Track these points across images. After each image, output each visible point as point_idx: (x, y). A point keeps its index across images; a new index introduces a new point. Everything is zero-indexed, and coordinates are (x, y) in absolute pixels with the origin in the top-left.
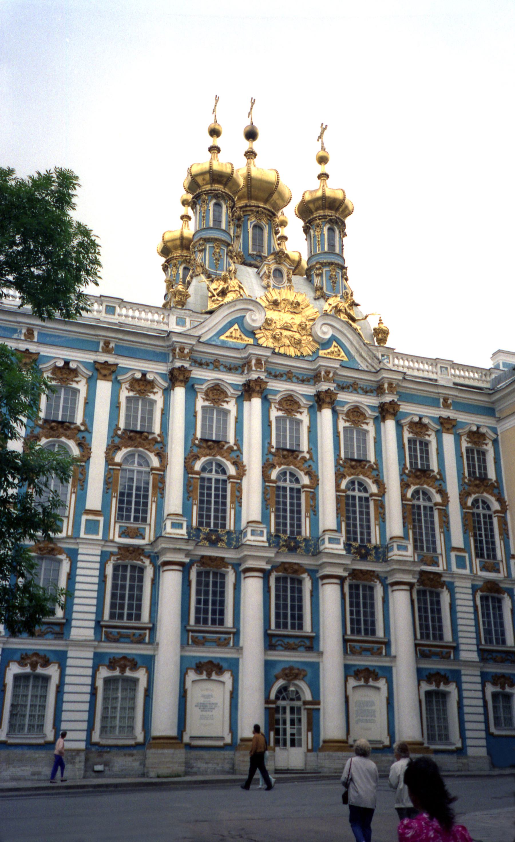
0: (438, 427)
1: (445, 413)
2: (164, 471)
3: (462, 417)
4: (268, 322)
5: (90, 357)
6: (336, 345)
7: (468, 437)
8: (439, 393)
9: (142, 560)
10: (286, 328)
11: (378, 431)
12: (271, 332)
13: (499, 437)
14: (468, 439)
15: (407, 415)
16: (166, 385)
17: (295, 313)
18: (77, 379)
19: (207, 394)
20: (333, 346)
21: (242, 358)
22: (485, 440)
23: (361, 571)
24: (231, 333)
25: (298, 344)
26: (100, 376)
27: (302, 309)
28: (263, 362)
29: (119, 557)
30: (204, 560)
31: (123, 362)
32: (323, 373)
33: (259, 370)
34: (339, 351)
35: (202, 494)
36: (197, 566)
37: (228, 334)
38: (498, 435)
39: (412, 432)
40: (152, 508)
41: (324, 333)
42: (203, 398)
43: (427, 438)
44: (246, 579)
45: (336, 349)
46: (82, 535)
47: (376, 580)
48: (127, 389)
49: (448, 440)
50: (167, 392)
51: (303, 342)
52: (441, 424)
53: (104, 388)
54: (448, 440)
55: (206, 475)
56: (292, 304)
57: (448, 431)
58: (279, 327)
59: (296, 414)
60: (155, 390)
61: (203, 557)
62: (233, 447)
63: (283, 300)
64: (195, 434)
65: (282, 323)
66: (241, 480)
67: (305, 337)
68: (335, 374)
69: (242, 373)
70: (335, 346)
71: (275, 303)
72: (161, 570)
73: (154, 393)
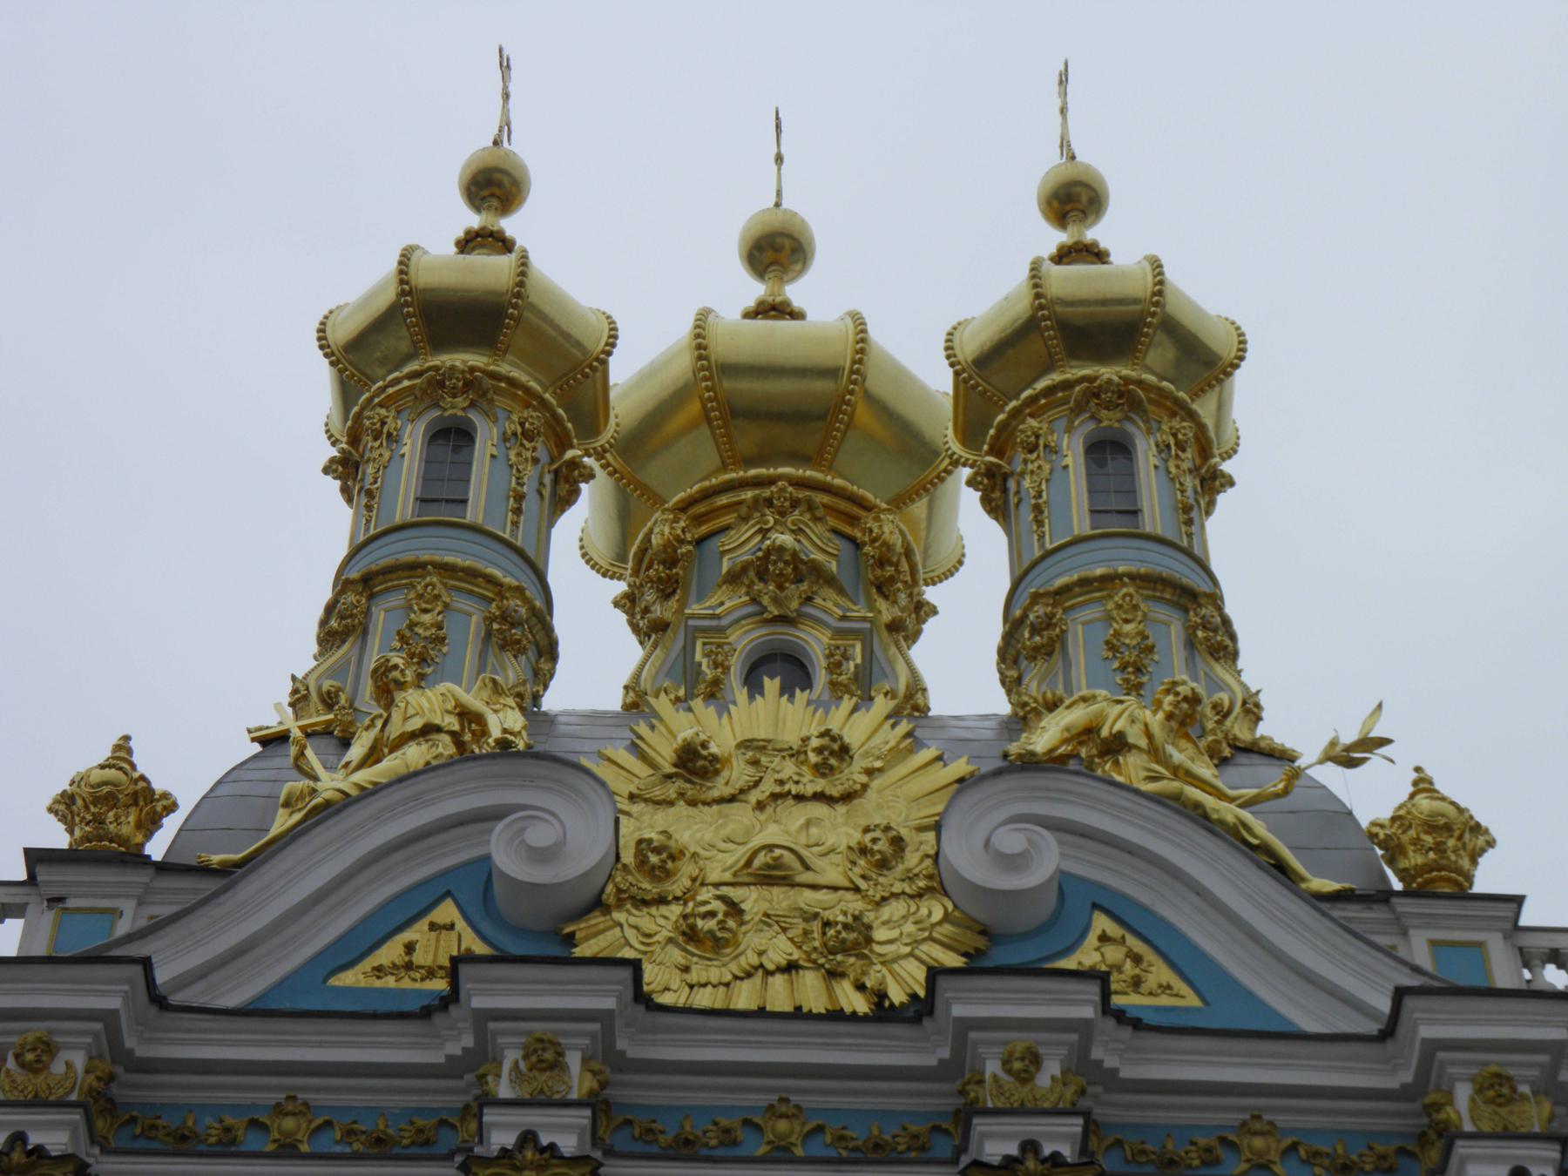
4: (658, 860)
6: (1113, 929)
10: (772, 875)
12: (675, 910)
17: (820, 797)
20: (1092, 939)
24: (410, 948)
25: (845, 948)
27: (870, 772)
32: (992, 1067)
34: (1137, 959)
37: (390, 953)
45: (1114, 954)
51: (880, 934)
56: (797, 754)
58: (714, 876)
63: (745, 745)
65: (739, 854)
67: (896, 908)
68: (1082, 1068)
70: (1104, 938)
71: (694, 764)
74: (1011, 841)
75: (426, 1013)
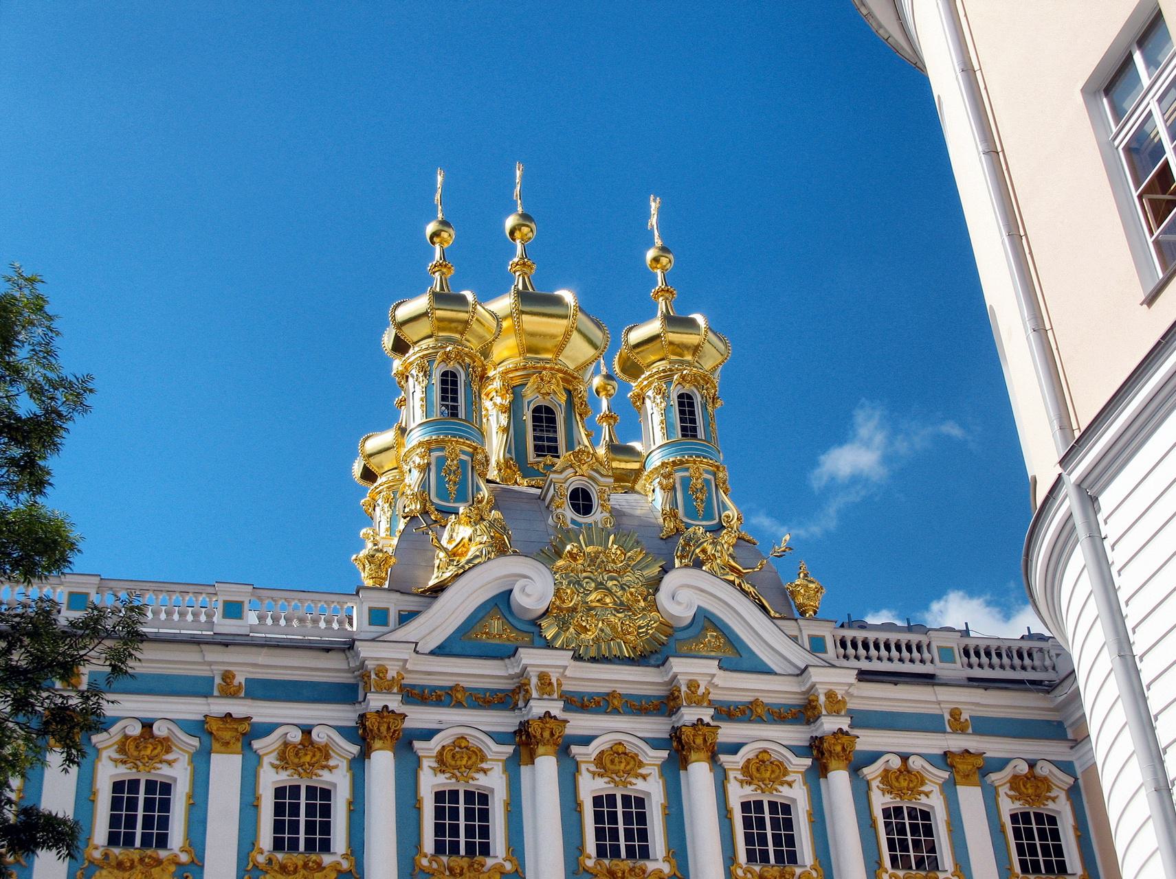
0: (946, 775)
1: (956, 743)
3: (994, 747)
5: (192, 709)
7: (1011, 788)
13: (1080, 781)
14: (1012, 793)
15: (873, 757)
16: (355, 749)
18: (170, 757)
19: (440, 759)
21: (511, 677)
22: (1049, 789)
26: (216, 746)
28: (554, 680)
31: (262, 712)
33: (545, 696)
38: (1076, 779)
42: (433, 769)
43: (923, 799)
48: (273, 765)
49: (970, 798)
50: (358, 764)
52: (952, 766)
54: (970, 798)
57: (967, 779)
59: (634, 781)
60: (331, 763)
62: (502, 866)
64: (418, 846)
69: (515, 707)
73: (330, 769)
75: (502, 659)
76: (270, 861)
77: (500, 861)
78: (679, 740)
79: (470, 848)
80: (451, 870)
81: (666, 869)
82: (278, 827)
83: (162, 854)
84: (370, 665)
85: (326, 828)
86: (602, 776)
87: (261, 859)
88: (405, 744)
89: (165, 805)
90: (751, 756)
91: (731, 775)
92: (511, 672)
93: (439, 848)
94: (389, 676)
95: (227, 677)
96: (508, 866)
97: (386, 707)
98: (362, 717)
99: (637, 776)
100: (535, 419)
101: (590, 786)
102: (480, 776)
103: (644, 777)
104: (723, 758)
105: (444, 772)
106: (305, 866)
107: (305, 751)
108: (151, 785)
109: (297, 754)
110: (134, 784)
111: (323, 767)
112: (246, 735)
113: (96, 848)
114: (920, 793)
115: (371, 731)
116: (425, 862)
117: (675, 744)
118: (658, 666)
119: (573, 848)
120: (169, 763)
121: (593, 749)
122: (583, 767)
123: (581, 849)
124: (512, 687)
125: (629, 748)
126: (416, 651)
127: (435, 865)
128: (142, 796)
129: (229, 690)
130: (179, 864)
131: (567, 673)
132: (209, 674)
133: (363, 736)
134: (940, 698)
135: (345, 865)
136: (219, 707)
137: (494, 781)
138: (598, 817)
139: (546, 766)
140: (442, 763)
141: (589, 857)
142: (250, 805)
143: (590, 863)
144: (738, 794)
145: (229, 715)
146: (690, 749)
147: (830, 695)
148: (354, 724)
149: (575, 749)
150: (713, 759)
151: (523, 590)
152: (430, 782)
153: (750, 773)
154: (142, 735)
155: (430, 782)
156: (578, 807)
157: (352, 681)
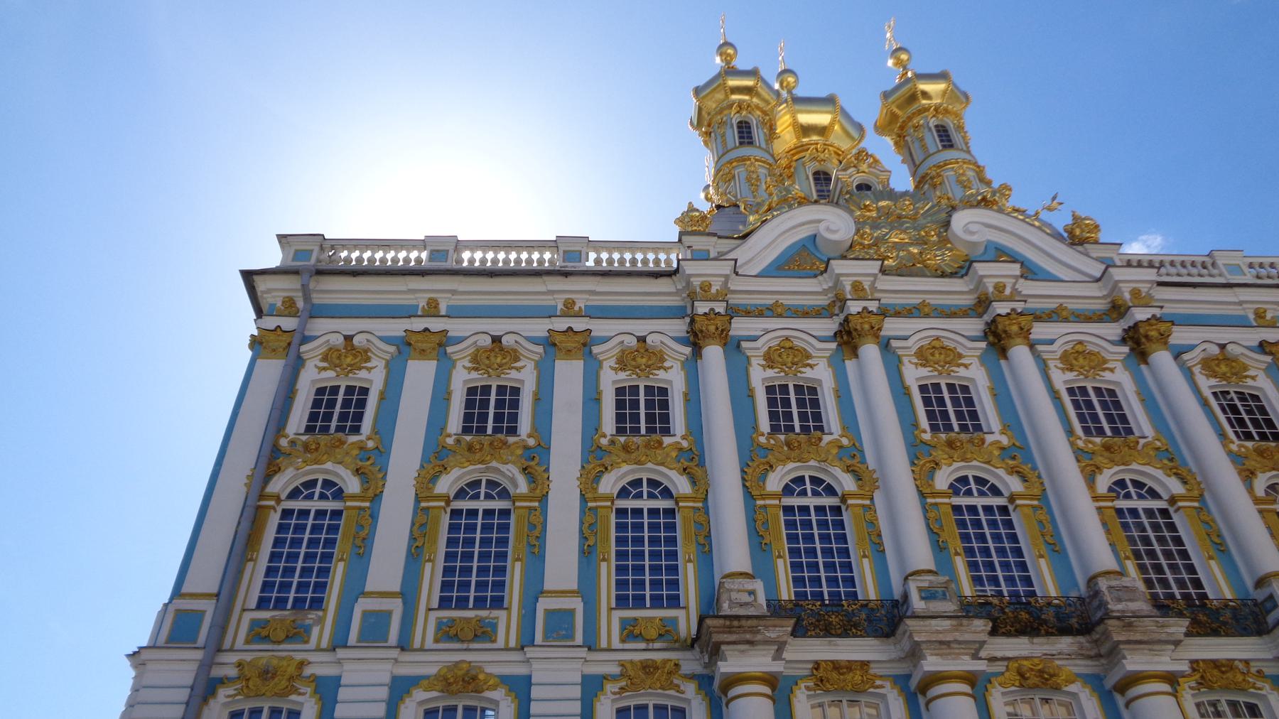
2: (705, 500)
8: (1241, 303)
9: (678, 686)
11: (1139, 381)
21: (825, 292)
23: (1215, 664)
29: (623, 683)
30: (821, 673)
32: (991, 289)
35: (792, 538)
36: (808, 688)
39: (1215, 377)
40: (689, 576)
41: (972, 233)
43: (1250, 382)
44: (932, 705)
46: (539, 638)
47: (1259, 684)
53: (569, 374)
55: (796, 501)
60: (666, 364)
61: (817, 665)
64: (755, 428)
66: (872, 499)
72: (724, 701)
73: (666, 369)
74: (973, 228)
75: (815, 276)
76: (612, 442)
77: (836, 436)
78: (995, 334)
79: (805, 429)
80: (788, 444)
81: (1005, 441)
82: (620, 418)
83: (511, 439)
84: (696, 282)
85: (665, 418)
86: (924, 366)
87: (604, 441)
88: (733, 347)
89: (515, 404)
90: (1068, 347)
91: (1051, 364)
92: (825, 287)
93: (775, 429)
94: (713, 290)
95: (569, 304)
96: (845, 441)
97: (712, 309)
98: (692, 321)
99: (959, 365)
100: (815, 179)
101: (914, 375)
102: (808, 370)
103: (966, 366)
104: (1040, 348)
105: (772, 367)
106: (647, 446)
107: (642, 355)
108: (501, 389)
109: (634, 359)
110: (486, 389)
111: (659, 368)
112: (584, 345)
113: (449, 436)
114: (1246, 377)
115: (702, 331)
116: (762, 440)
117: (991, 338)
118: (962, 277)
119: (909, 425)
120: (518, 369)
121: (913, 344)
122: (905, 360)
123: (916, 425)
124: (827, 303)
125: (946, 343)
126: (737, 274)
127: (772, 442)
128: (493, 398)
129: (569, 310)
130: (526, 448)
131: (879, 286)
132: (553, 303)
133: (695, 340)
134: (1242, 298)
135: (685, 444)
136: (561, 324)
137: (821, 374)
138: (927, 401)
139: (870, 351)
140: (770, 360)
141: (925, 432)
142: (592, 399)
143: (927, 436)
144: (1061, 379)
145: (570, 329)
146: (1009, 336)
147: (1136, 293)
148: (685, 335)
149: (894, 343)
150: (1032, 346)
151: (828, 229)
152: (759, 376)
153: (1069, 360)
154: (492, 350)
155: (759, 376)
156: (907, 392)
157: (681, 304)
